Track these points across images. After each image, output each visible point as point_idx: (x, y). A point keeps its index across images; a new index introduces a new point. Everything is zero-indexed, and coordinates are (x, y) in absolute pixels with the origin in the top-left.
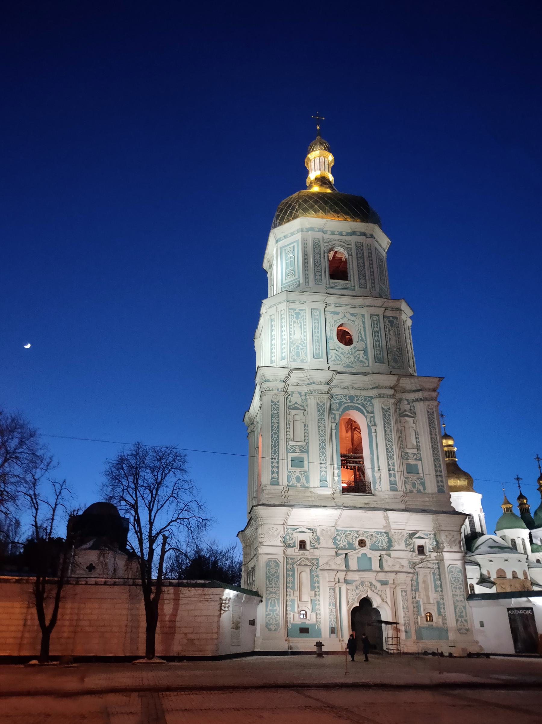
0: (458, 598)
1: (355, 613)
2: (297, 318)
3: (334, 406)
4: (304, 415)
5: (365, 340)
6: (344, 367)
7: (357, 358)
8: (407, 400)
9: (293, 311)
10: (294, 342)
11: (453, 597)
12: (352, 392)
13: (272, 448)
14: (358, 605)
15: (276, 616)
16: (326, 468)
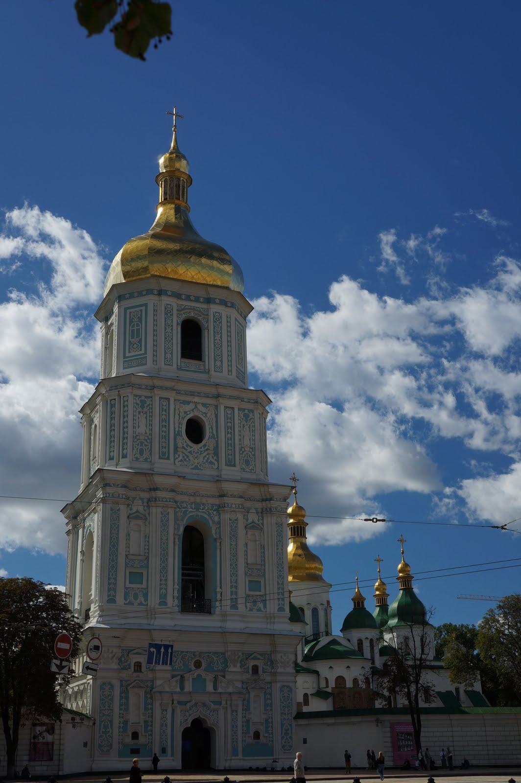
1: (186, 734)
2: (143, 407)
5: (216, 437)
6: (191, 469)
7: (206, 458)
8: (256, 509)
9: (138, 397)
10: (138, 437)
11: (281, 716)
12: (198, 499)
13: (110, 563)
14: (190, 726)
15: (108, 738)
16: (166, 585)
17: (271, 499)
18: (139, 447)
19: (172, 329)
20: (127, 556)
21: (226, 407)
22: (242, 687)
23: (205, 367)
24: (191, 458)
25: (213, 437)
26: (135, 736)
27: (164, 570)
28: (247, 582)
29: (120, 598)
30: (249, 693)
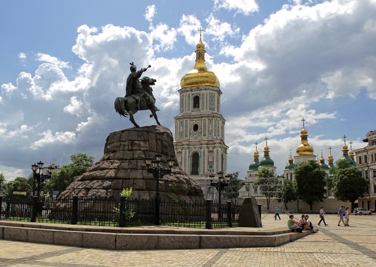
2: (181, 124)
8: (212, 147)
17: (215, 144)
21: (204, 120)
24: (194, 135)
25: (201, 129)
28: (209, 166)
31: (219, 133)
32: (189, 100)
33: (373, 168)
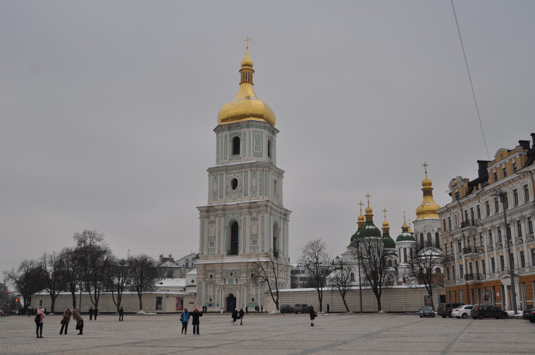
0: (262, 293)
2: (215, 179)
3: (226, 219)
4: (215, 225)
8: (256, 212)
12: (233, 212)
16: (220, 246)
18: (214, 195)
19: (227, 145)
20: (208, 237)
22: (247, 283)
23: (240, 156)
26: (211, 300)
27: (219, 241)
29: (205, 253)
30: (250, 284)
31: (267, 190)
32: (226, 143)
33: (457, 238)
